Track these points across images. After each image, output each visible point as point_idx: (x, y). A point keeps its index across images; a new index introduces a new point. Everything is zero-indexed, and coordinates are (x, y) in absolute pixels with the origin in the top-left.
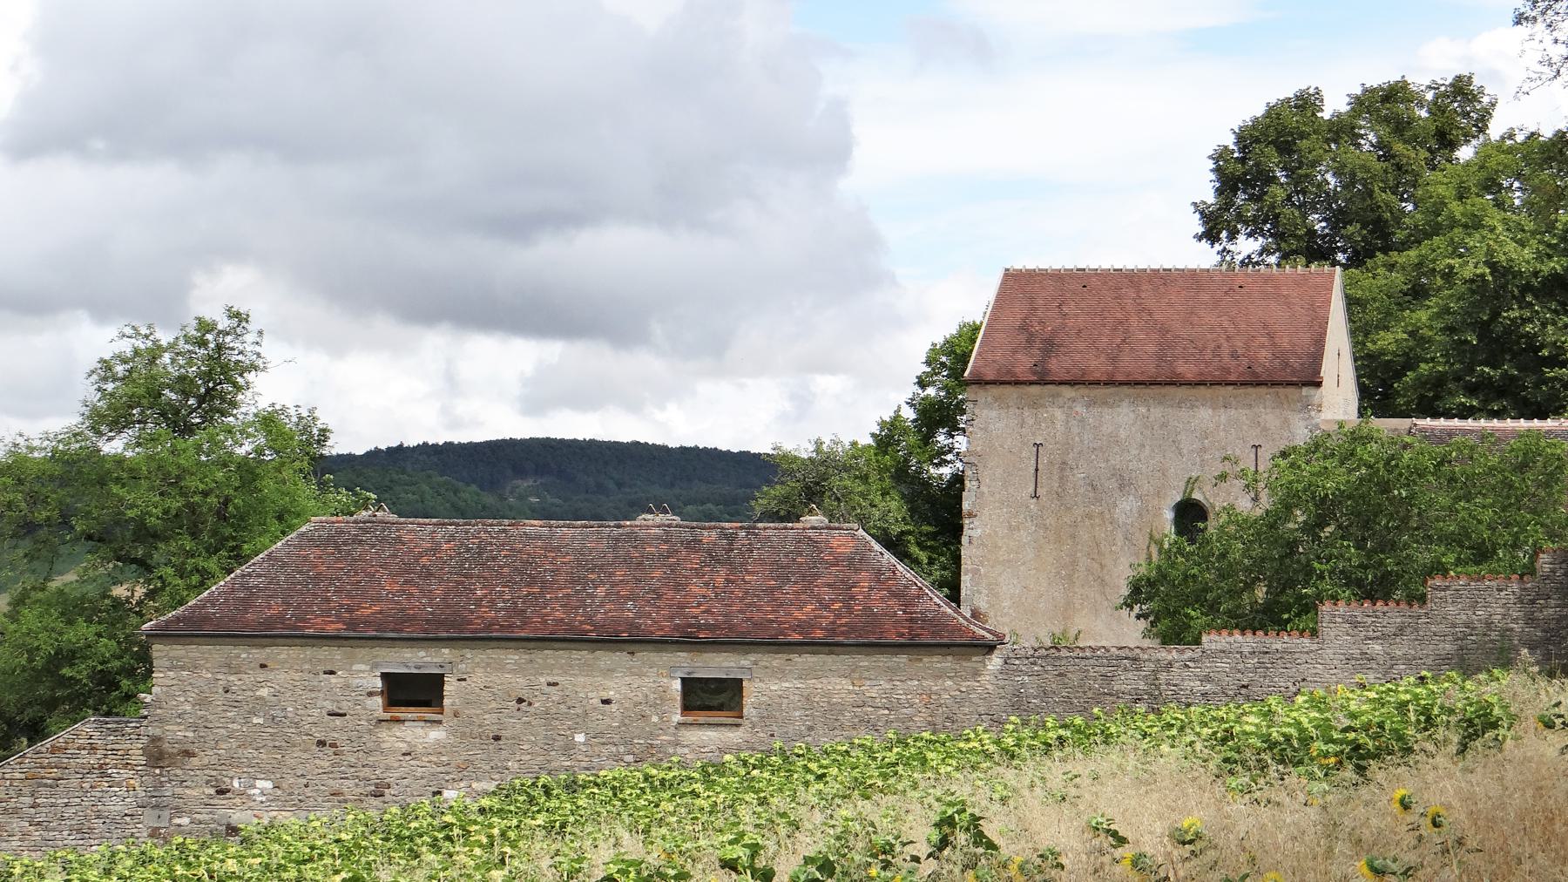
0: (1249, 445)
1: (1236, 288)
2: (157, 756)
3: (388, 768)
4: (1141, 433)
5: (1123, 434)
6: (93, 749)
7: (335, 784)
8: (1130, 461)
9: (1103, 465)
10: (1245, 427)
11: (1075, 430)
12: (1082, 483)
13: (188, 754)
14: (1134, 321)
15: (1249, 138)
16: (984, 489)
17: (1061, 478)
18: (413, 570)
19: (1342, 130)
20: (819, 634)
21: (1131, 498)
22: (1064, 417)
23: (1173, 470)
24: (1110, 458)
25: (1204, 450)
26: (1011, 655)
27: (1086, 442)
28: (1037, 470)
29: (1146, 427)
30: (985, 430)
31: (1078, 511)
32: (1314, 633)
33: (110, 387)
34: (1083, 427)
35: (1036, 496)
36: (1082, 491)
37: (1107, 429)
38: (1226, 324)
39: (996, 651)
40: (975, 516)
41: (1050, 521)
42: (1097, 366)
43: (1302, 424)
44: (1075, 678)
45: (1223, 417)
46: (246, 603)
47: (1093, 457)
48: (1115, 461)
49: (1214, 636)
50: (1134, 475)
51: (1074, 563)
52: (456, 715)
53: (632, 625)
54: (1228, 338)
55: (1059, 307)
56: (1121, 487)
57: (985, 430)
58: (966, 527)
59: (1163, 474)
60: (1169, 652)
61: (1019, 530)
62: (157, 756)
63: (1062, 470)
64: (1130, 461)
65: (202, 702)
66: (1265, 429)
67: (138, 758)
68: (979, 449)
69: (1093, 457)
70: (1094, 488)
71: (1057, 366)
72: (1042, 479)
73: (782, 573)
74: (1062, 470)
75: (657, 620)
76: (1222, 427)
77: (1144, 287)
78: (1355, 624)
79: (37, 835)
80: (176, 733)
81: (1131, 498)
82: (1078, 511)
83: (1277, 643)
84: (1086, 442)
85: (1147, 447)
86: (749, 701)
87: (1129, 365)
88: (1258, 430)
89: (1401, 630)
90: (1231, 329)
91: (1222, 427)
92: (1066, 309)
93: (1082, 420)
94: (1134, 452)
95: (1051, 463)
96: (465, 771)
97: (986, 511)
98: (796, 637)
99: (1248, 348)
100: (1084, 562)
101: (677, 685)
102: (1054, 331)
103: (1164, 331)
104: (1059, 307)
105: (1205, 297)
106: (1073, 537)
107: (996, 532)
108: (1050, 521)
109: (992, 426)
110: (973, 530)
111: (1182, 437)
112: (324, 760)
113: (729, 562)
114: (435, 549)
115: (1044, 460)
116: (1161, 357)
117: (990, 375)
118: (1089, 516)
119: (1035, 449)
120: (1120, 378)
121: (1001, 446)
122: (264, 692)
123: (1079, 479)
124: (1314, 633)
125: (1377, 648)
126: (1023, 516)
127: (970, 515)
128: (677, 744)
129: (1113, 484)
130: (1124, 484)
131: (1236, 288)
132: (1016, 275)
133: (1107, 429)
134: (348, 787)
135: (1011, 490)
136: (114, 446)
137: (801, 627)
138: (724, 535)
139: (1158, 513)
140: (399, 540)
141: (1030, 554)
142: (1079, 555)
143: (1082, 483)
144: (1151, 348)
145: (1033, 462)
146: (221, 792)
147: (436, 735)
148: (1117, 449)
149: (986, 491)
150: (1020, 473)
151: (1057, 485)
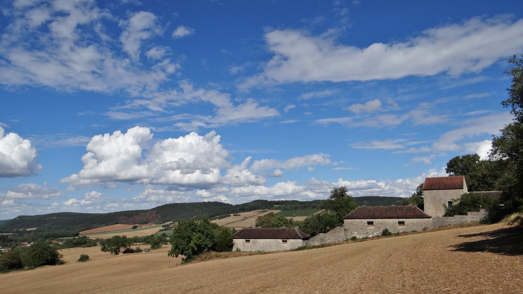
2: (345, 230)
3: (368, 231)
5: (441, 194)
6: (339, 229)
7: (363, 233)
13: (348, 230)
15: (451, 161)
18: (369, 211)
19: (462, 161)
20: (412, 217)
32: (467, 215)
33: (332, 194)
41: (434, 204)
42: (437, 187)
44: (440, 220)
46: (353, 215)
49: (456, 215)
52: (375, 225)
53: (392, 216)
62: (345, 230)
65: (349, 225)
67: (343, 230)
70: (438, 200)
71: (433, 188)
72: (432, 200)
73: (408, 210)
75: (394, 216)
78: (471, 214)
79: (334, 238)
80: (347, 228)
83: (463, 216)
86: (405, 224)
89: (477, 215)
93: (436, 193)
95: (433, 198)
96: (376, 231)
98: (410, 217)
101: (398, 222)
103: (444, 183)
105: (449, 180)
108: (434, 204)
110: (425, 205)
112: (362, 230)
113: (402, 209)
114: (371, 209)
115: (432, 198)
120: (440, 189)
122: (355, 224)
124: (467, 215)
125: (474, 216)
128: (398, 228)
129: (440, 200)
130: (442, 200)
134: (364, 233)
136: (333, 199)
137: (410, 216)
138: (401, 207)
140: (367, 208)
141: (432, 207)
144: (443, 185)
146: (352, 233)
147: (373, 227)
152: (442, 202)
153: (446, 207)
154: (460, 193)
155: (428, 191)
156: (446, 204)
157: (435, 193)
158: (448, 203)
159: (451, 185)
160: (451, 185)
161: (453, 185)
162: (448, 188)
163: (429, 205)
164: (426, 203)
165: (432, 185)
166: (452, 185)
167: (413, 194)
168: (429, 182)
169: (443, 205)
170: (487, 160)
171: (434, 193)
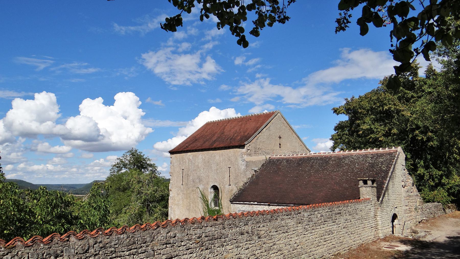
5: (200, 165)
9: (196, 175)
11: (190, 165)
25: (217, 169)
31: (191, 189)
35: (182, 185)
37: (196, 164)
41: (185, 192)
43: (241, 159)
50: (202, 178)
51: (190, 205)
63: (188, 176)
66: (231, 162)
74: (188, 176)
82: (191, 189)
85: (205, 169)
88: (230, 162)
94: (202, 171)
95: (185, 175)
100: (192, 205)
106: (190, 197)
109: (174, 165)
111: (212, 165)
115: (184, 174)
118: (193, 191)
129: (197, 181)
133: (196, 164)
141: (181, 202)
142: (191, 203)
148: (199, 170)
153: (208, 202)
154: (236, 159)
157: (189, 160)
163: (178, 194)
169: (201, 196)
171: (187, 161)
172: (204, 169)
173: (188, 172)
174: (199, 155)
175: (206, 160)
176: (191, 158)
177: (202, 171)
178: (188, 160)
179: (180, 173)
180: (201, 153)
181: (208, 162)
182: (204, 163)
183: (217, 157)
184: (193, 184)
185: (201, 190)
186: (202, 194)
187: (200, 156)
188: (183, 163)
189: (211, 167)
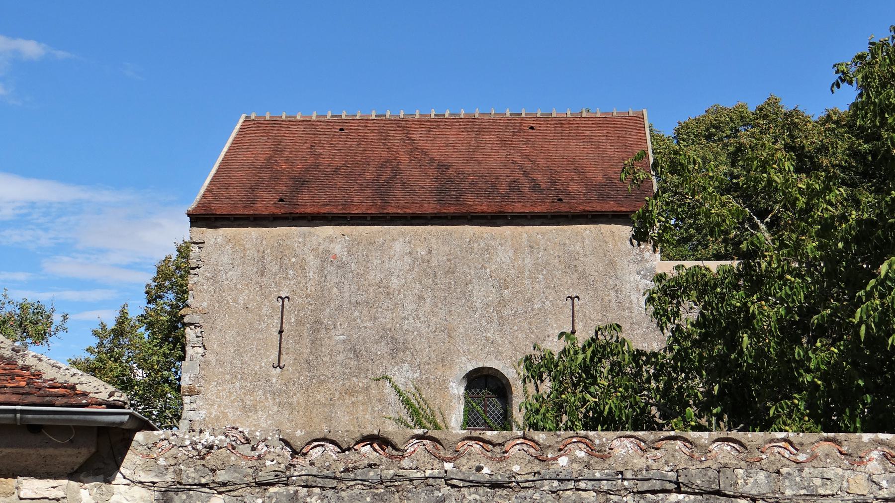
0: (563, 297)
1: (527, 129)
4: (420, 283)
5: (395, 283)
8: (404, 318)
9: (369, 324)
10: (557, 273)
11: (333, 279)
12: (341, 347)
14: (404, 158)
16: (211, 357)
17: (313, 342)
21: (406, 367)
22: (317, 262)
23: (462, 330)
24: (379, 315)
25: (502, 303)
26: (190, 474)
27: (347, 294)
28: (281, 332)
29: (425, 274)
30: (214, 280)
31: (335, 386)
34: (344, 276)
36: (340, 358)
37: (374, 276)
38: (519, 160)
39: (130, 458)
40: (198, 393)
41: (298, 398)
42: (361, 203)
43: (633, 267)
45: (528, 261)
47: (357, 314)
48: (385, 319)
50: (410, 337)
54: (526, 174)
55: (311, 148)
56: (393, 354)
57: (214, 280)
58: (186, 407)
59: (449, 336)
60: (855, 459)
61: (256, 411)
63: (315, 331)
64: (404, 318)
66: (584, 275)
68: (205, 304)
69: (357, 314)
70: (357, 354)
71: (306, 203)
72: (289, 343)
74: (315, 331)
76: (527, 273)
77: (412, 130)
81: (406, 367)
82: (335, 386)
84: (347, 294)
85: (428, 300)
87: (399, 202)
88: (576, 275)
90: (529, 165)
91: (527, 273)
92: (319, 150)
93: (342, 266)
94: (410, 307)
95: (299, 322)
97: (213, 387)
99: (553, 182)
102: (307, 170)
103: (443, 167)
104: (311, 148)
107: (225, 415)
109: (222, 275)
111: (474, 287)
115: (291, 318)
116: (441, 191)
117: (222, 209)
118: (350, 392)
119: (280, 303)
120: (392, 210)
121: (235, 300)
123: (337, 342)
126: (261, 392)
127: (192, 392)
129: (383, 349)
131: (527, 129)
132: (258, 122)
133: (374, 276)
135: (246, 358)
139: (442, 385)
143: (341, 347)
144: (428, 183)
145: (277, 320)
148: (387, 303)
149: (213, 361)
150: (259, 336)
151: (308, 350)
152: (403, 376)
154: (612, 264)
155: (253, 233)
156: (435, 401)
157: (326, 257)
158: (458, 389)
159: (514, 186)
160: (514, 186)
161: (536, 187)
162: (484, 208)
164: (211, 390)
165: (300, 183)
166: (525, 183)
167: (111, 325)
168: (278, 149)
170: (752, 109)
171: (312, 261)
172: (422, 298)
173: (319, 309)
174: (394, 240)
175: (434, 262)
176: (338, 249)
177: (410, 307)
178: (317, 256)
179: (264, 312)
180: (404, 234)
181: (449, 272)
182: (425, 274)
183: (503, 256)
184: (353, 363)
185: (402, 388)
186: (407, 402)
187: (398, 246)
188: (284, 269)
189: (466, 295)
